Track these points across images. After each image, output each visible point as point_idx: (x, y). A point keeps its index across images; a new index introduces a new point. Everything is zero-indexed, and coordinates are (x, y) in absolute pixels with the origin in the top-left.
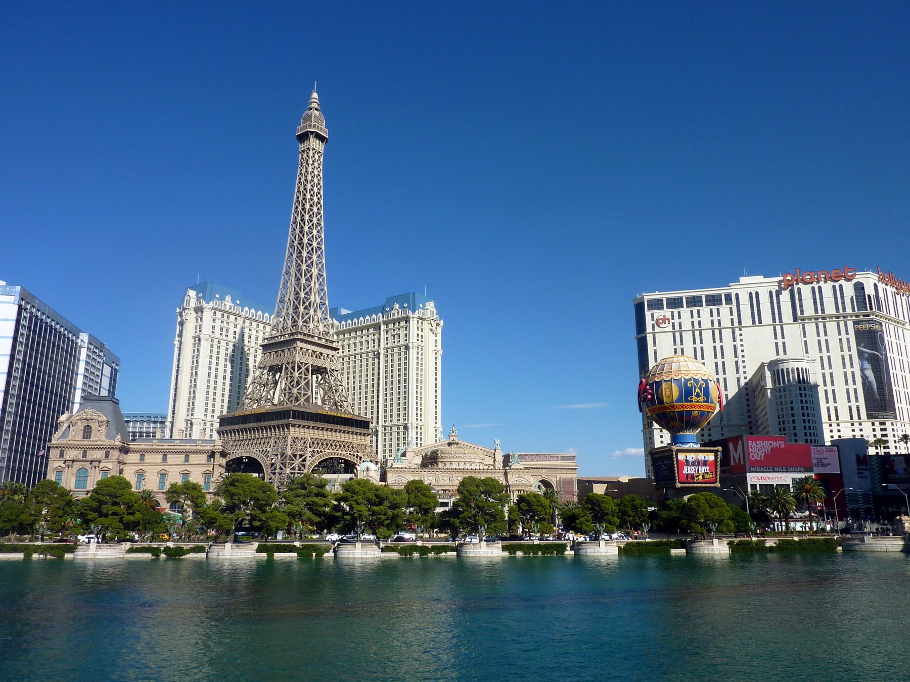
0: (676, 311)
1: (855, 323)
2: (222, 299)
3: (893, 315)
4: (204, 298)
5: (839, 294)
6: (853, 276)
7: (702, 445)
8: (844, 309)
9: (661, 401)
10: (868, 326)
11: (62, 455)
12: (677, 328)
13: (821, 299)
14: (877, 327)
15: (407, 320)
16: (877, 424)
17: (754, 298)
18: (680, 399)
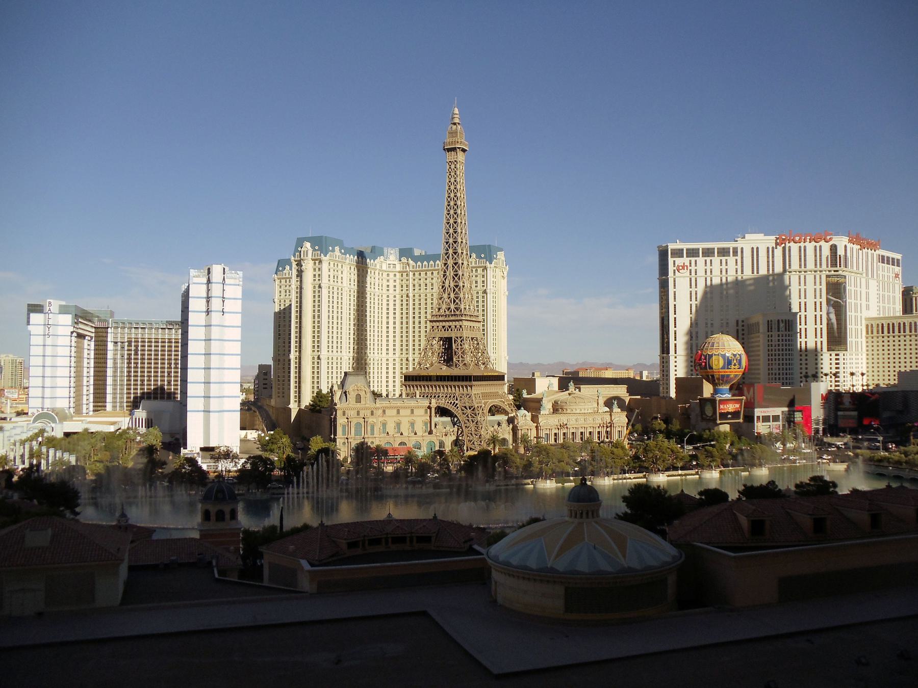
0: (693, 259)
1: (828, 276)
2: (333, 251)
3: (855, 268)
4: (321, 250)
5: (818, 251)
6: (831, 239)
7: (733, 396)
8: (821, 265)
9: (711, 368)
10: (836, 279)
11: (344, 414)
12: (693, 273)
13: (805, 256)
14: (841, 280)
15: (485, 268)
16: (833, 355)
17: (755, 252)
18: (723, 368)
